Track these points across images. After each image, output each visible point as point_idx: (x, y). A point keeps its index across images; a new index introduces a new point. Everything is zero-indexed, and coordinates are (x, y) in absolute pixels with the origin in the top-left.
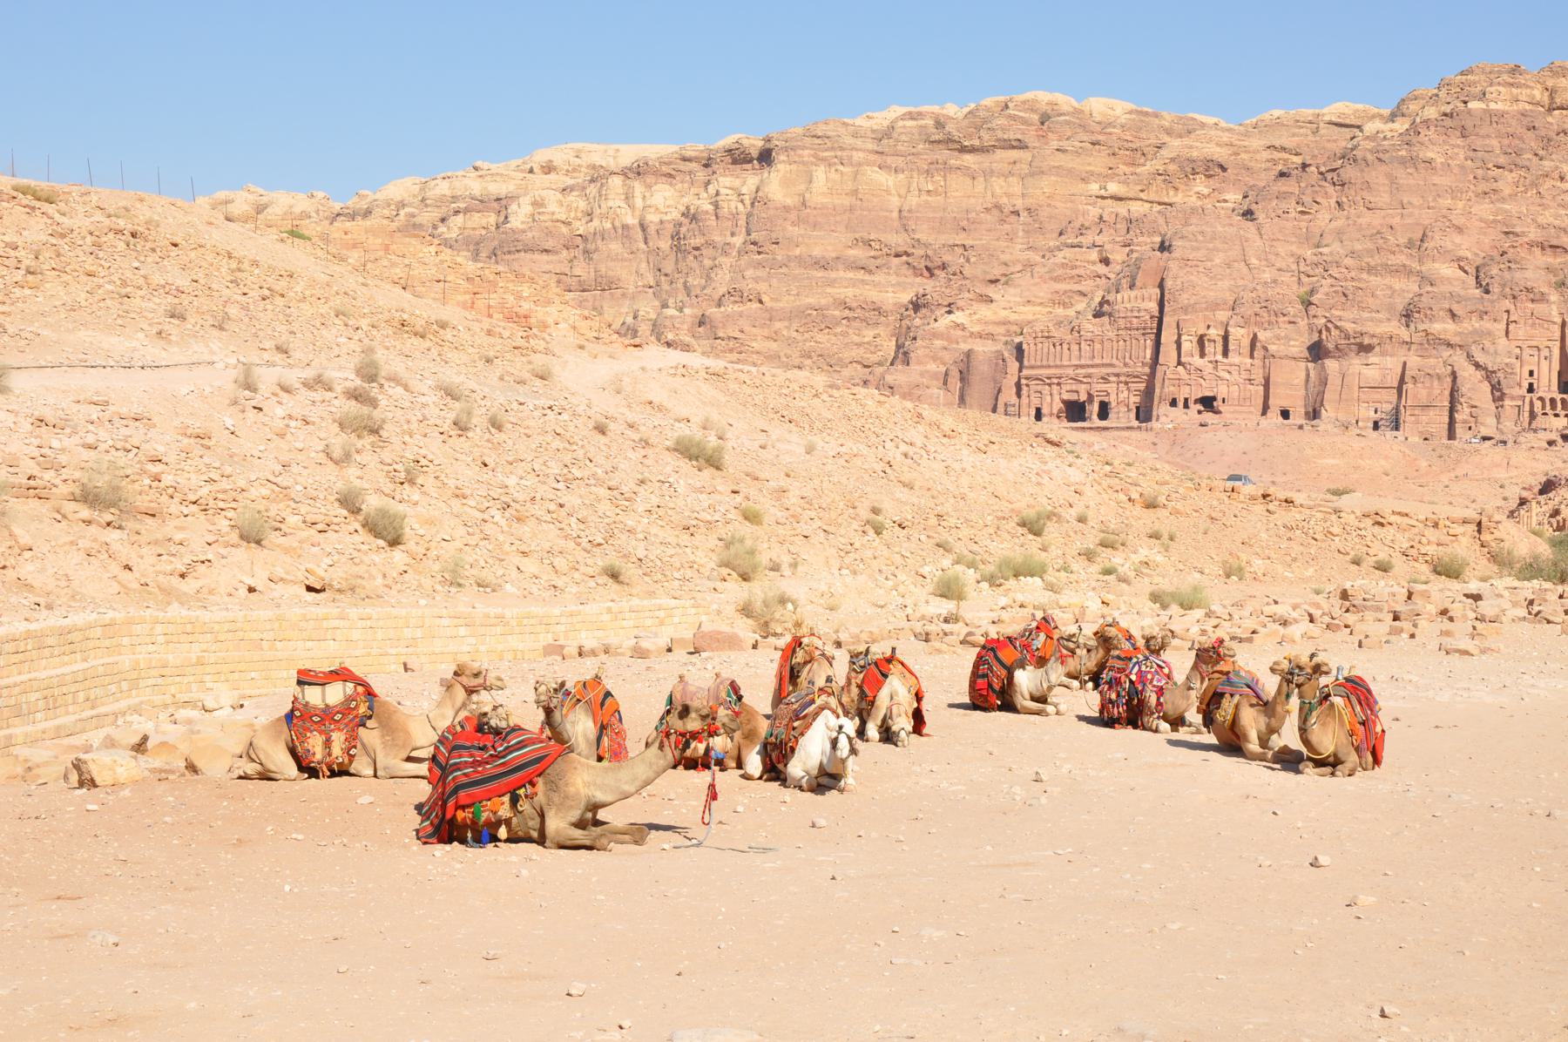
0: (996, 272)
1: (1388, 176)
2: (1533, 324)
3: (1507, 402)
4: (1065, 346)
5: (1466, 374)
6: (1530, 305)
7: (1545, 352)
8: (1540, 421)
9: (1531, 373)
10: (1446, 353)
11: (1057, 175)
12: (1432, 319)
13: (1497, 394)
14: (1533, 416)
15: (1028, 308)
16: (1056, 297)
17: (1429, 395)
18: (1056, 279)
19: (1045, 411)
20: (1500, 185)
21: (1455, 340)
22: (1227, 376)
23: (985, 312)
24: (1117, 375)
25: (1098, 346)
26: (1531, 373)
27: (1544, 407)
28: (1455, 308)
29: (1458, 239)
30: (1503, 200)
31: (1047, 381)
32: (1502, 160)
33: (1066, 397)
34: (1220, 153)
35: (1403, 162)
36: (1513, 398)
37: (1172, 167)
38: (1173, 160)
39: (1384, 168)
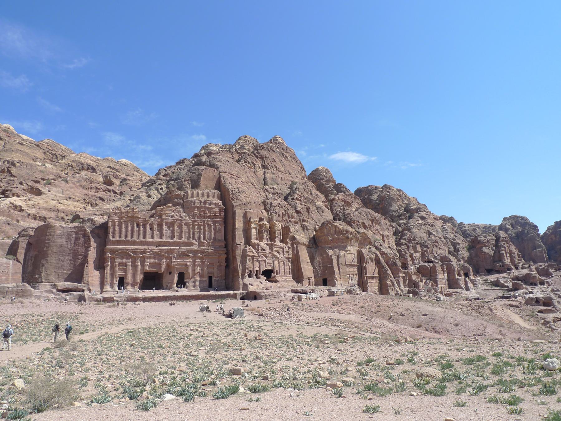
0: (38, 176)
4: (148, 226)
11: (20, 154)
15: (69, 202)
16: (87, 198)
18: (83, 187)
19: (129, 279)
22: (278, 255)
23: (36, 199)
24: (195, 252)
25: (176, 228)
31: (132, 256)
33: (147, 268)
34: (92, 164)
37: (74, 164)
38: (74, 161)
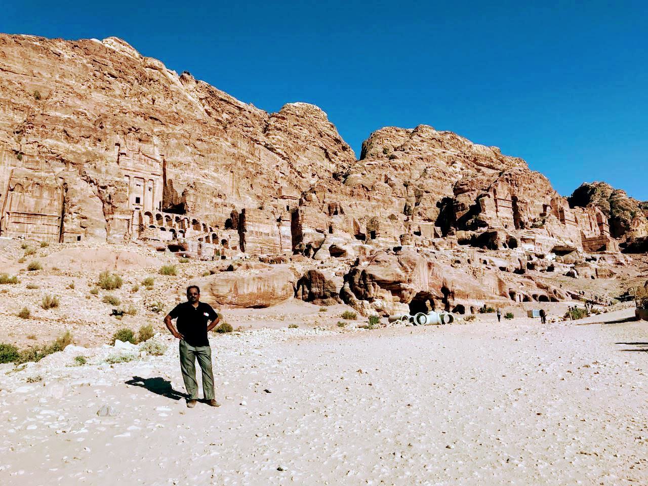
1: (22, 54)
2: (140, 159)
3: (117, 216)
5: (78, 188)
6: (137, 143)
7: (150, 184)
8: (147, 233)
9: (138, 200)
10: (60, 169)
12: (45, 135)
13: (108, 207)
14: (142, 228)
17: (37, 204)
20: (112, 86)
21: (70, 157)
26: (138, 200)
27: (152, 222)
28: (69, 130)
29: (79, 102)
30: (115, 97)
32: (114, 73)
35: (35, 48)
36: (122, 212)
39: (20, 48)
